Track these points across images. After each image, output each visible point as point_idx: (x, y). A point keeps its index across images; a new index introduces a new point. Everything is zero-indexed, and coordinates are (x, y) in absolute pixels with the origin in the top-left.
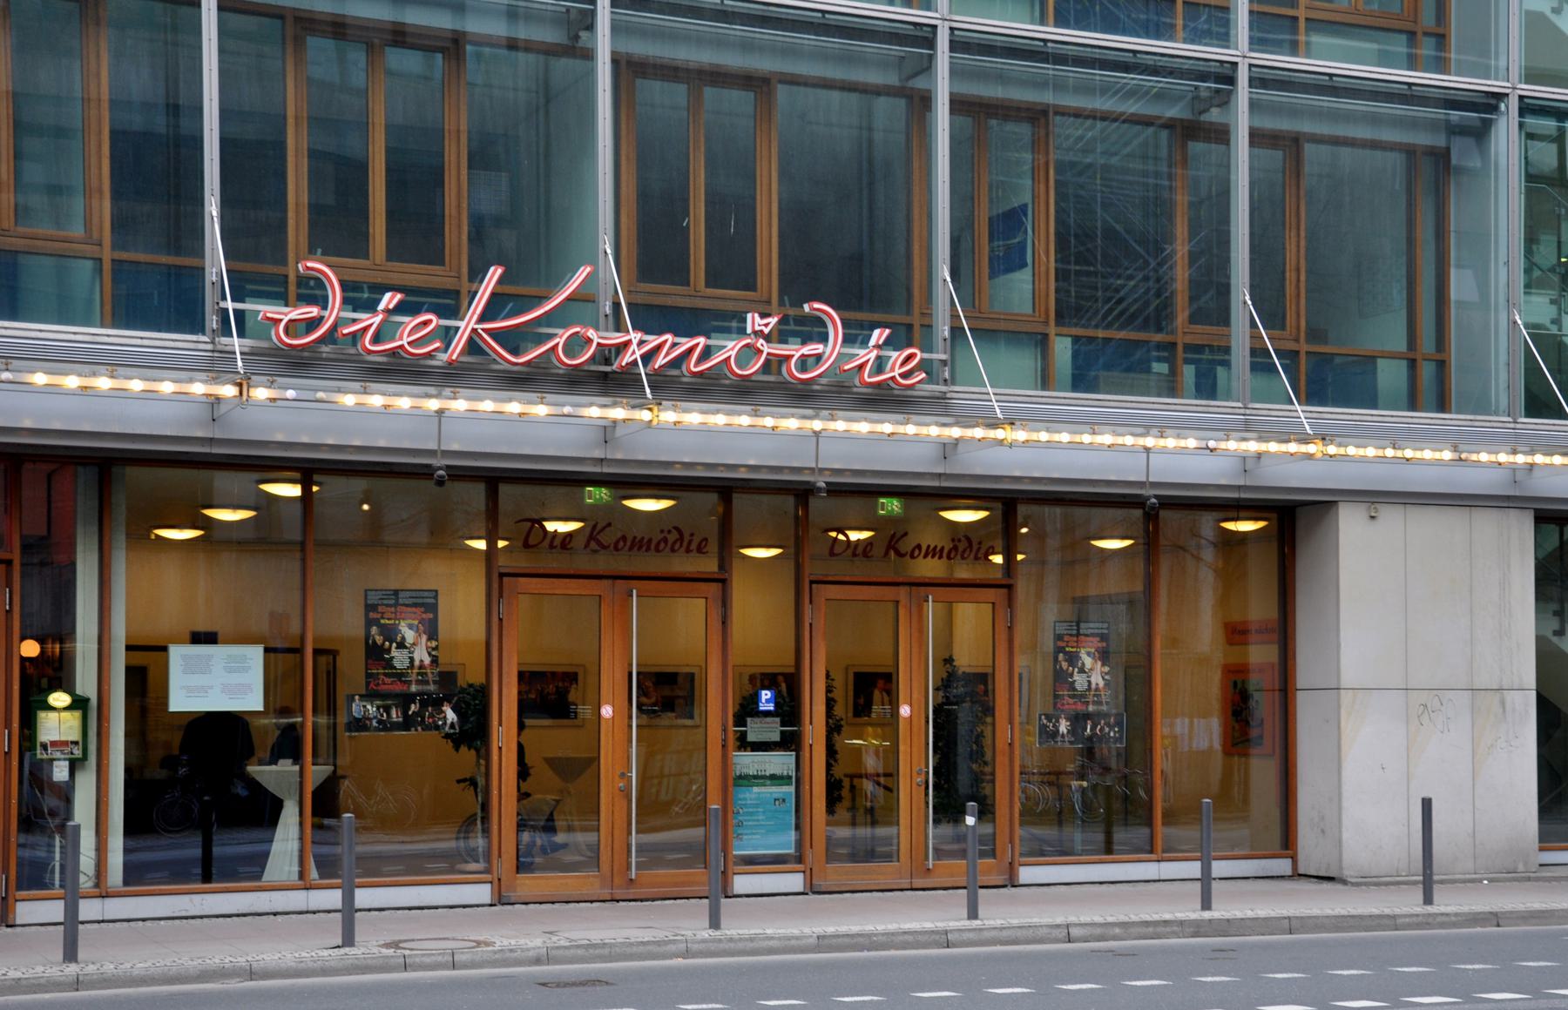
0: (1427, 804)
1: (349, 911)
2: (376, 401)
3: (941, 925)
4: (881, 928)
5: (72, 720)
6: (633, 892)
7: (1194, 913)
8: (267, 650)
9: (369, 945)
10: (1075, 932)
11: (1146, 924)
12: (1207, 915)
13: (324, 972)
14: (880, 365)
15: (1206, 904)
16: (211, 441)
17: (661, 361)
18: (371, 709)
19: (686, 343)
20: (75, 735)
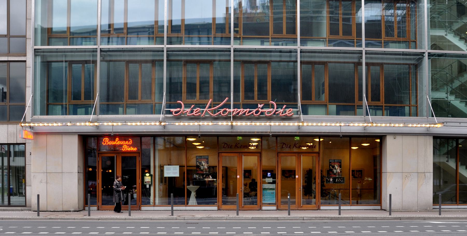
0: (38, 196)
1: (172, 210)
2: (191, 124)
3: (277, 216)
4: (264, 216)
5: (150, 177)
6: (243, 209)
7: (337, 216)
8: (180, 166)
9: (175, 216)
10: (305, 218)
11: (320, 217)
12: (340, 216)
13: (163, 220)
14: (192, 112)
15: (340, 214)
16: (165, 132)
17: (240, 114)
18: (197, 176)
19: (245, 110)
20: (150, 181)
